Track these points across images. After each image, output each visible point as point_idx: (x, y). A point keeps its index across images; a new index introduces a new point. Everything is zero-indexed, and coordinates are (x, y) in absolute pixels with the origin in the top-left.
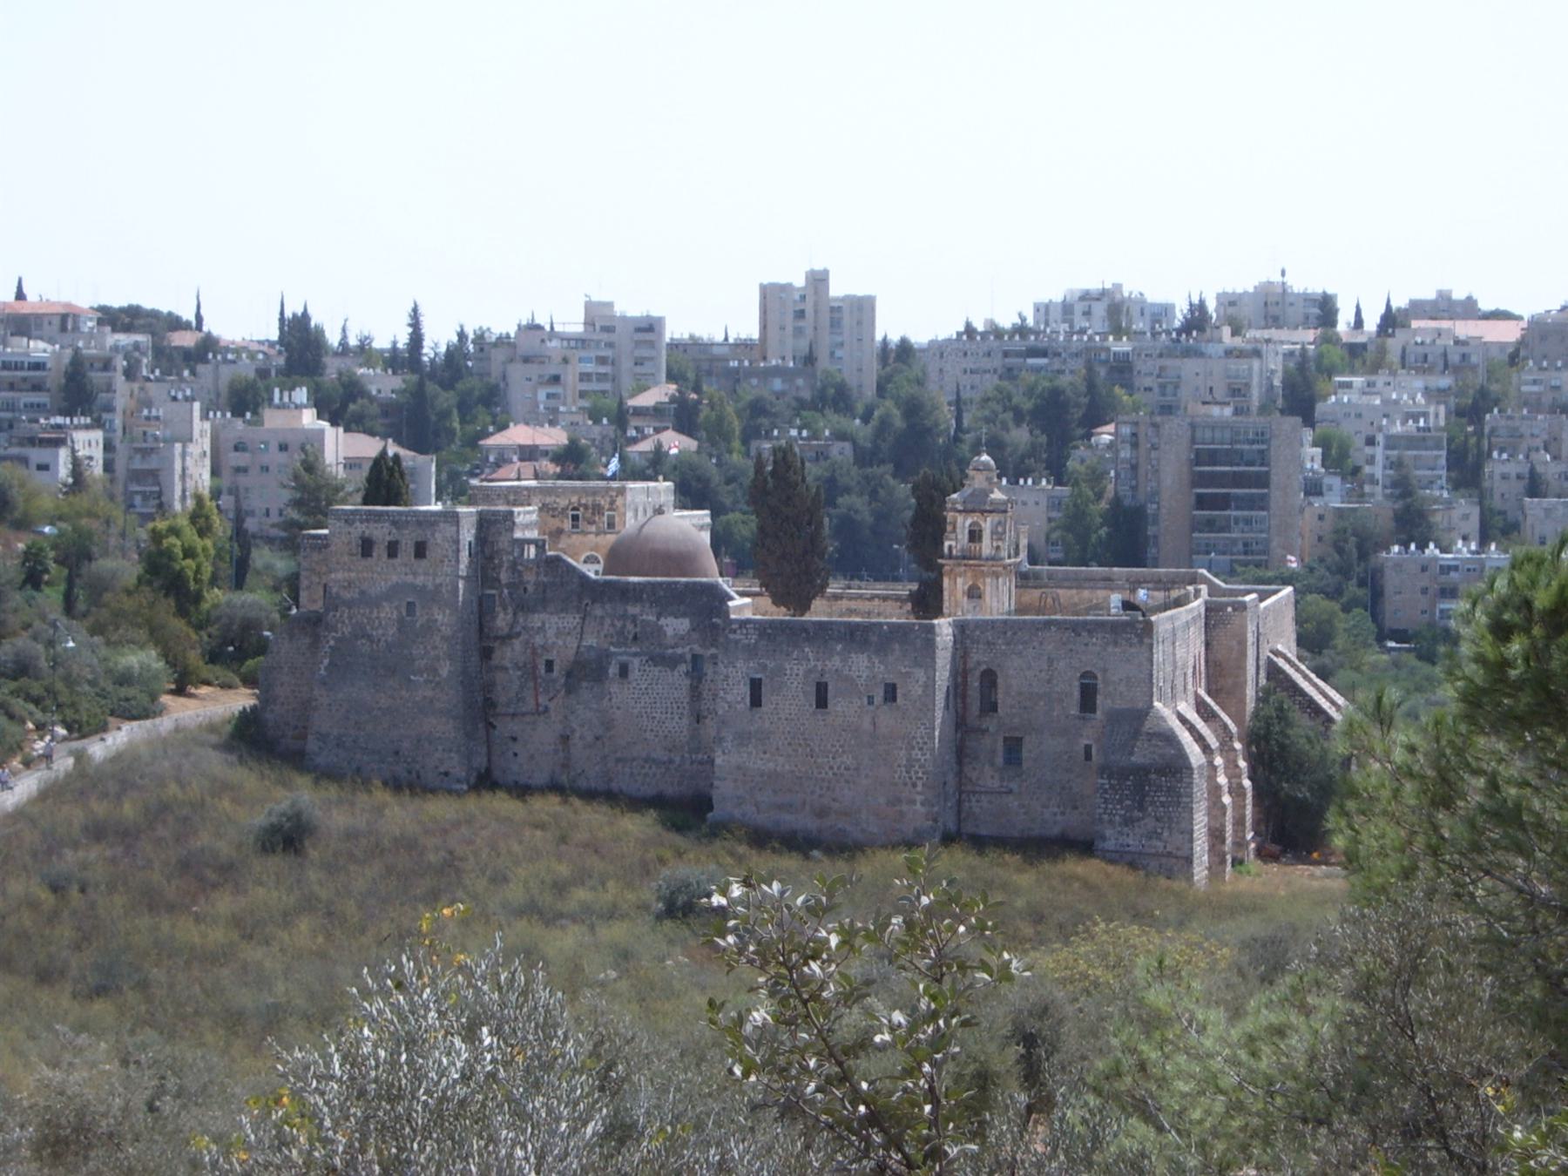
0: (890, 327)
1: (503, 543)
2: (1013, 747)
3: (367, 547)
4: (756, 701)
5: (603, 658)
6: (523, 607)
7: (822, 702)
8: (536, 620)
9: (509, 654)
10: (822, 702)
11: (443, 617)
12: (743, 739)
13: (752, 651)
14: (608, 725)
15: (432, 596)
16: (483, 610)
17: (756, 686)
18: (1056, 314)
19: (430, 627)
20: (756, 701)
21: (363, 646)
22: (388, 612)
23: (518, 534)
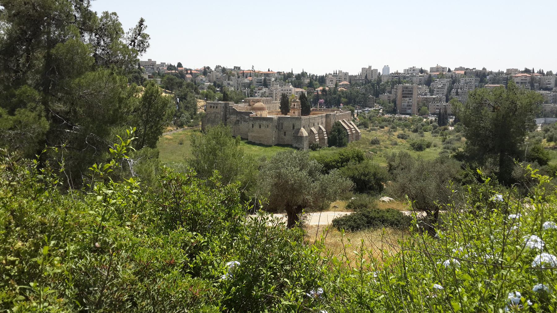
0: (350, 74)
1: (228, 106)
2: (285, 133)
3: (211, 107)
4: (253, 127)
5: (238, 121)
6: (230, 115)
7: (260, 127)
8: (232, 116)
9: (228, 120)
10: (260, 127)
11: (219, 116)
12: (252, 132)
13: (252, 121)
14: (239, 129)
15: (218, 113)
16: (225, 115)
17: (253, 125)
18: (406, 71)
19: (218, 117)
20: (253, 127)
21: (211, 119)
22: (213, 115)
23: (230, 105)
